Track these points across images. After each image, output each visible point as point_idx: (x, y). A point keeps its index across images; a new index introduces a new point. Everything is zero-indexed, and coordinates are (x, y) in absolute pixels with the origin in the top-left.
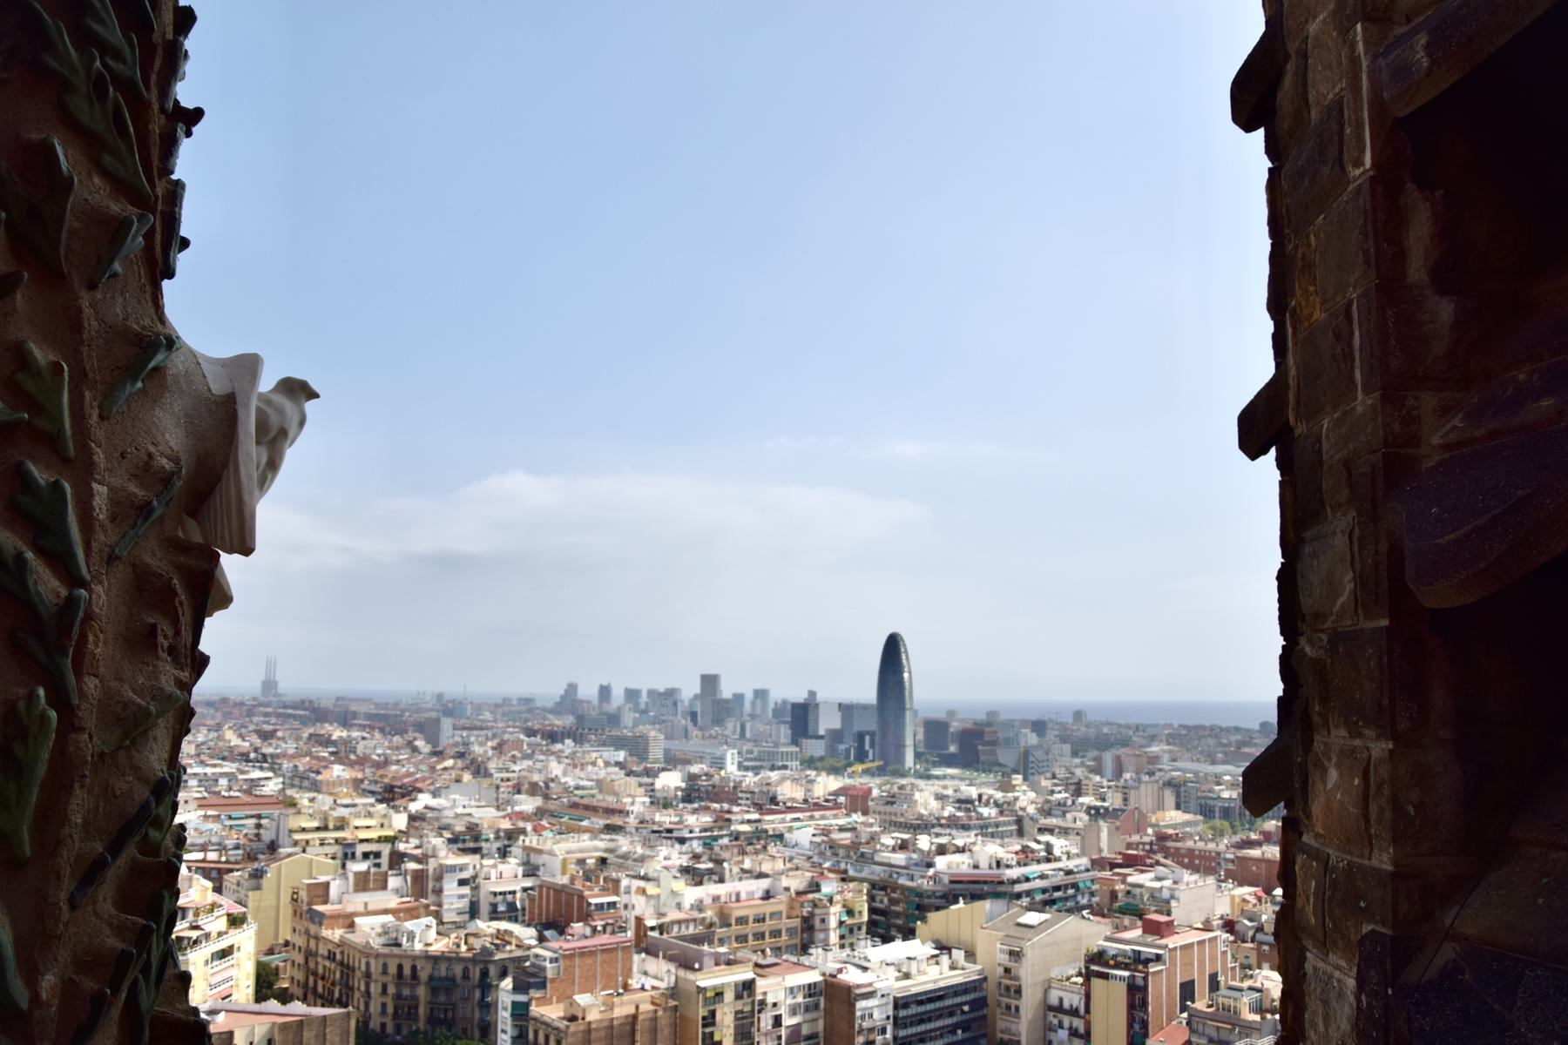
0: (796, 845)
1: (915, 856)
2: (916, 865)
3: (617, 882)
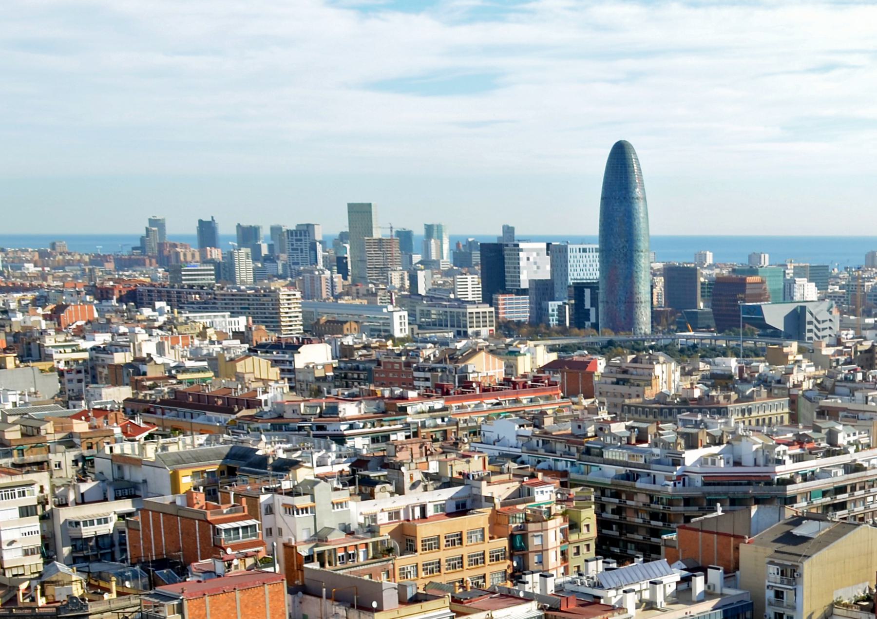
0: (499, 440)
1: (657, 451)
2: (659, 462)
3: (253, 500)
